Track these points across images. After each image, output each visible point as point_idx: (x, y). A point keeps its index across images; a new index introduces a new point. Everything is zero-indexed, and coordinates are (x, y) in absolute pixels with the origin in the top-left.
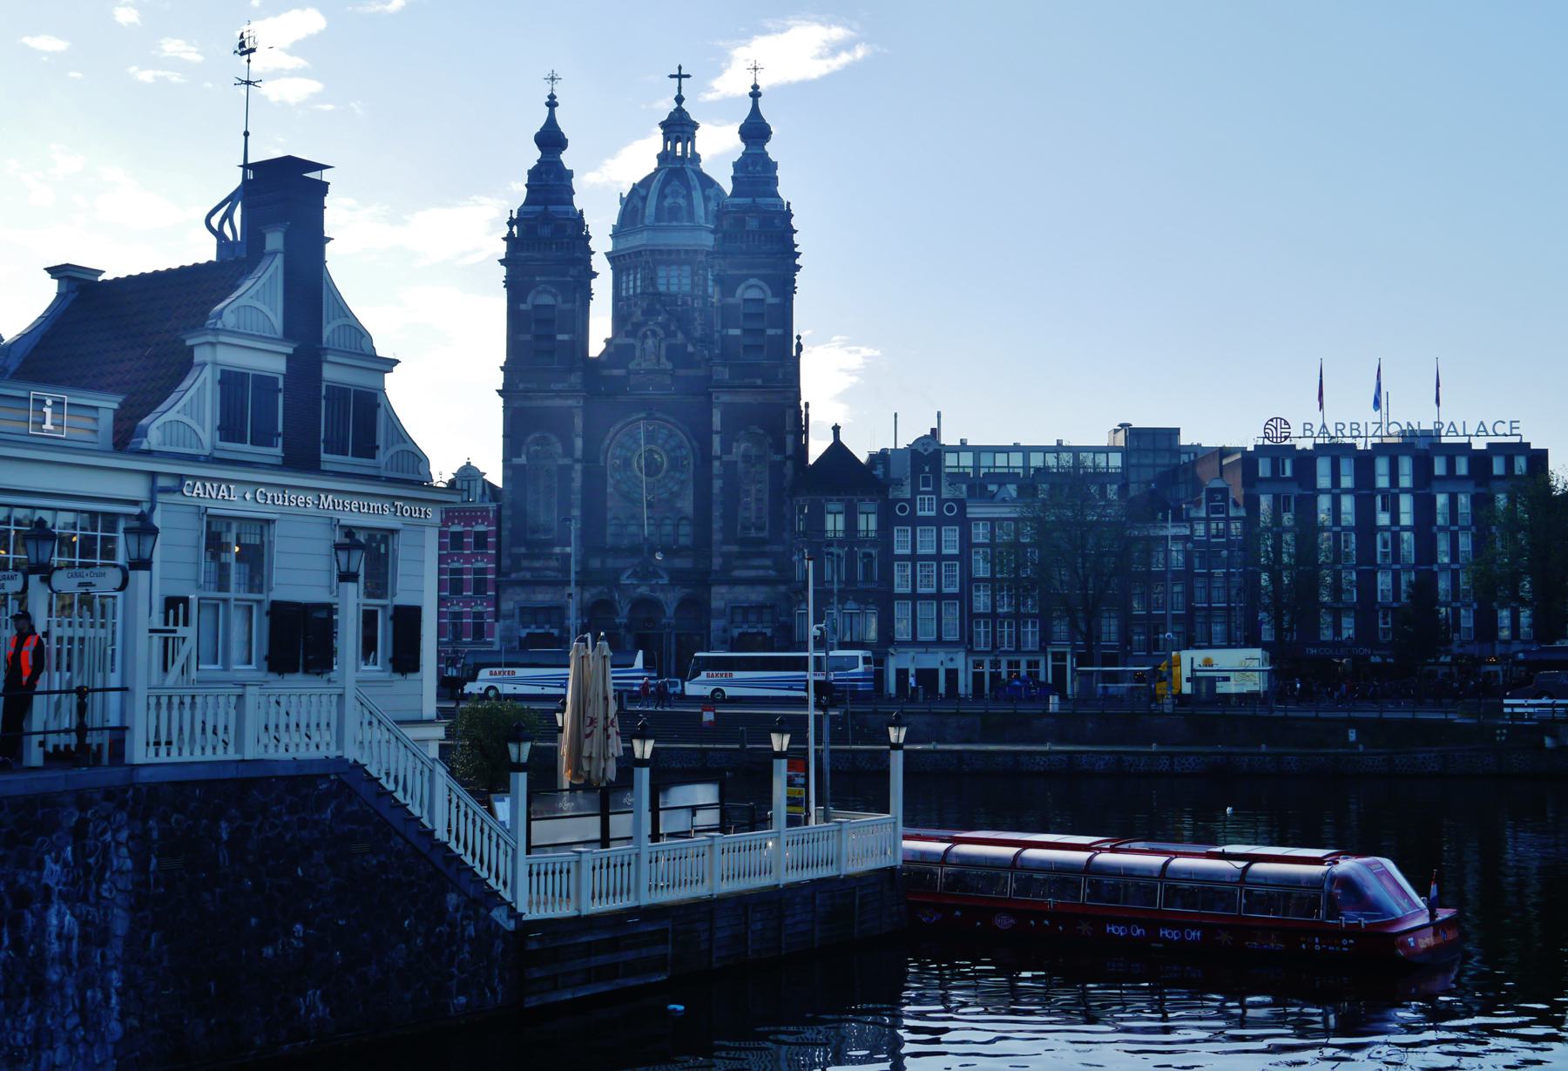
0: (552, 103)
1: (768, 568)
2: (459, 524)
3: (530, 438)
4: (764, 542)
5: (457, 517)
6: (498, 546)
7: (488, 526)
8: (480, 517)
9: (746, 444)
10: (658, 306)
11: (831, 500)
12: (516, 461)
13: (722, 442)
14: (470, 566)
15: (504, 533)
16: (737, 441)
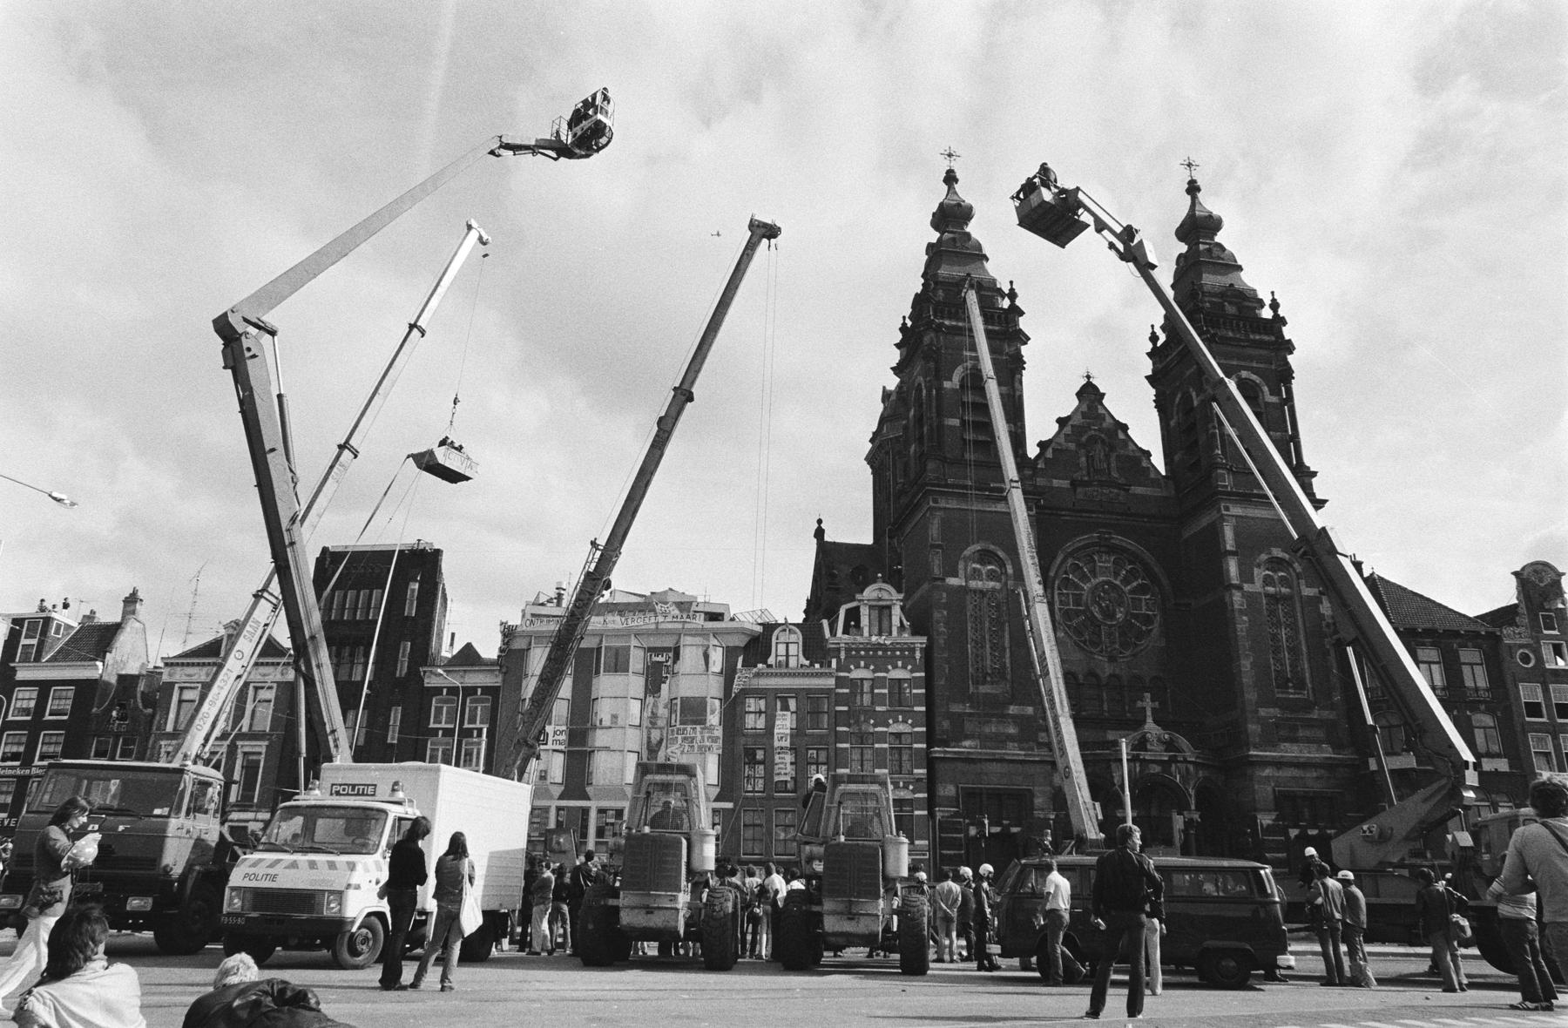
0: (950, 178)
1: (1319, 742)
2: (867, 667)
3: (967, 553)
4: (1308, 706)
5: (862, 658)
6: (929, 700)
7: (912, 671)
8: (899, 658)
9: (1267, 572)
10: (1101, 411)
11: (1423, 644)
12: (952, 581)
13: (1240, 565)
14: (885, 729)
15: (940, 682)
16: (1259, 566)
